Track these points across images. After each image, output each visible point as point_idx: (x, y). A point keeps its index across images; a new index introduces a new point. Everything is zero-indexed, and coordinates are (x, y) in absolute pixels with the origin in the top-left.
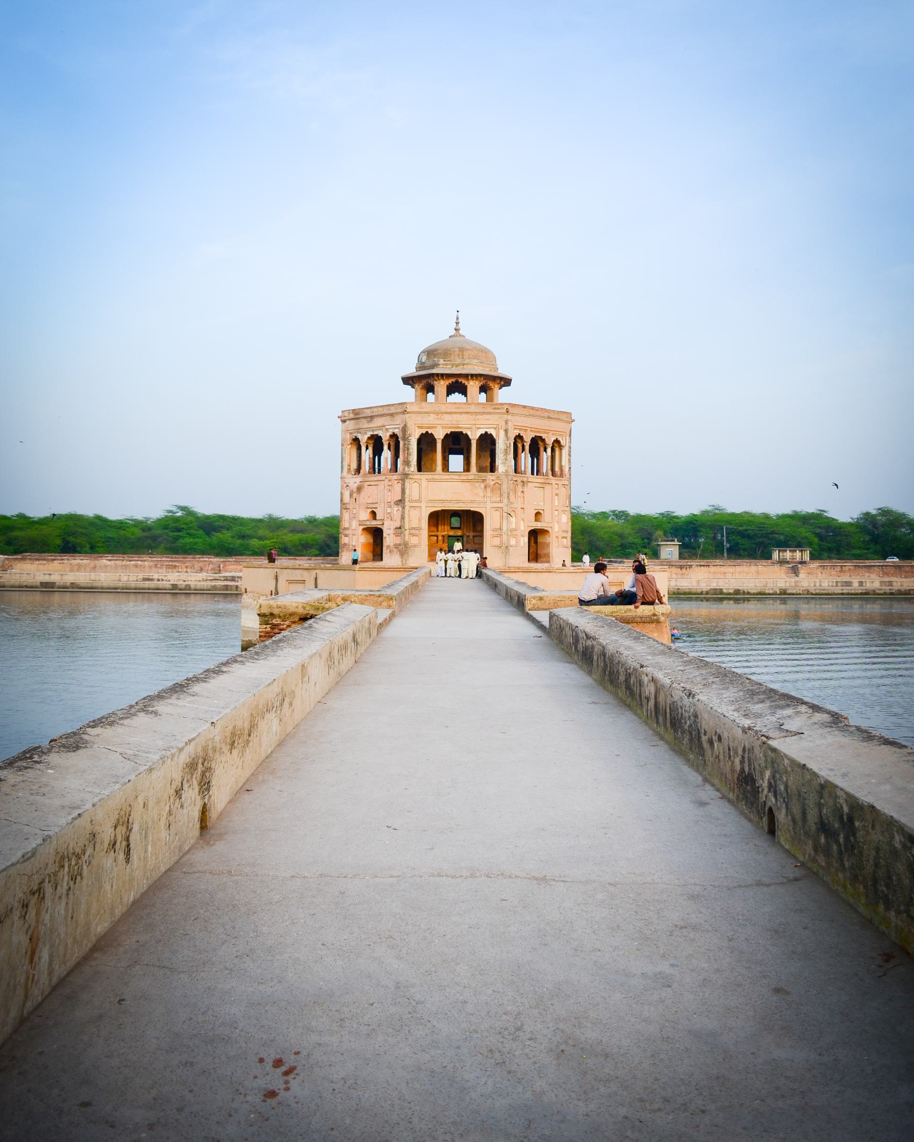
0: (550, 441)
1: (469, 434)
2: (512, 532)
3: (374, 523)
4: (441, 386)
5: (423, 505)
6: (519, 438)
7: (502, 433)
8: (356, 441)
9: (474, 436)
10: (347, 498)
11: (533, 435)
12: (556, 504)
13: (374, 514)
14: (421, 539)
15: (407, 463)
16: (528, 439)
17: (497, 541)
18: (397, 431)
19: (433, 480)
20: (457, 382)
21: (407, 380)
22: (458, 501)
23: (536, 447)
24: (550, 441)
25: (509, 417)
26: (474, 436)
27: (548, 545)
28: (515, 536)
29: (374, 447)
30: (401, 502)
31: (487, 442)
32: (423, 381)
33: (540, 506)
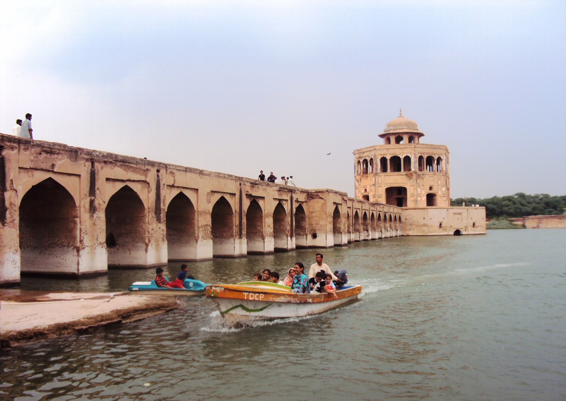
0: (436, 157)
1: (400, 156)
2: (419, 195)
3: (366, 194)
4: (393, 139)
5: (383, 185)
6: (421, 158)
7: (413, 155)
8: (359, 162)
9: (402, 157)
10: (357, 185)
11: (428, 155)
12: (440, 183)
13: (366, 190)
14: (383, 200)
15: (376, 170)
16: (425, 157)
17: (412, 199)
18: (372, 157)
19: (387, 176)
20: (399, 136)
21: (382, 136)
22: (396, 183)
23: (430, 161)
24: (436, 157)
25: (416, 149)
26: (402, 157)
27: (435, 200)
28: (420, 196)
29: (365, 164)
30: (374, 185)
31: (407, 159)
32: (386, 137)
33: (431, 184)
